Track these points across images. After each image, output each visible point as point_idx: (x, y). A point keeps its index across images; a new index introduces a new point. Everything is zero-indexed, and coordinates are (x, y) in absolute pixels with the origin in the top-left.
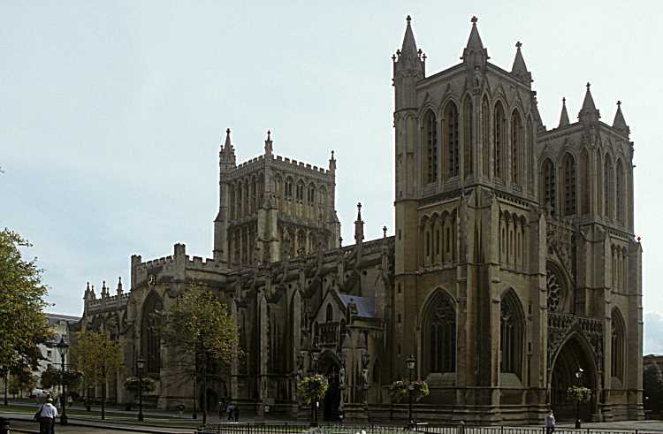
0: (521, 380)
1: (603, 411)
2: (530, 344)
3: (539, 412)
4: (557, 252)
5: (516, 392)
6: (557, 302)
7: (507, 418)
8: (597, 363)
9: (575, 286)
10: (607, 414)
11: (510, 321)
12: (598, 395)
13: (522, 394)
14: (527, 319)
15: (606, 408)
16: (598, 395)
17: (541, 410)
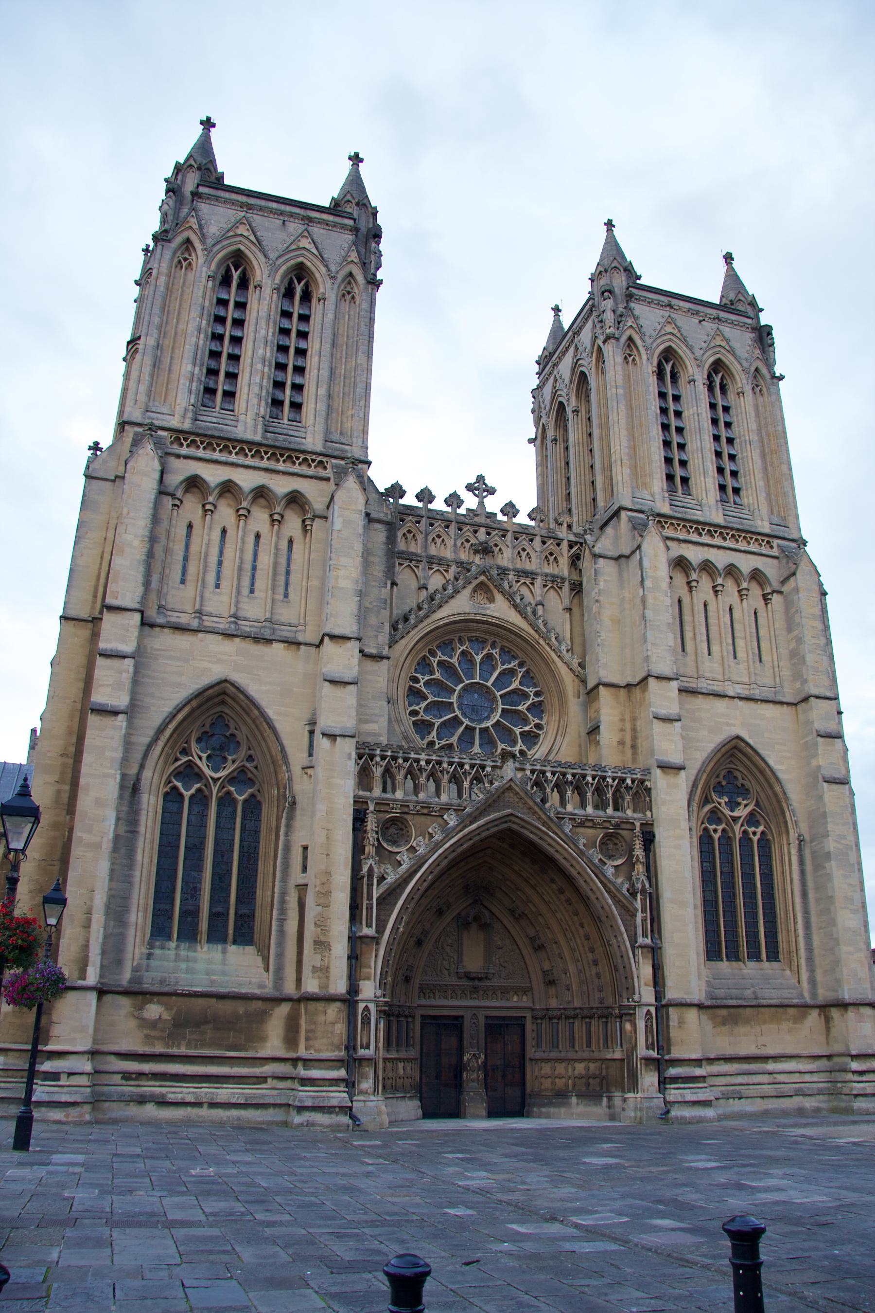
0: (267, 969)
1: (663, 1082)
2: (305, 848)
3: (311, 1082)
4: (503, 593)
5: (241, 1008)
6: (531, 738)
7: (171, 1097)
8: (629, 913)
9: (584, 681)
10: (673, 1094)
11: (240, 778)
12: (641, 1024)
13: (262, 1017)
14: (296, 770)
15: (673, 1071)
16: (641, 1024)
17: (315, 1073)
